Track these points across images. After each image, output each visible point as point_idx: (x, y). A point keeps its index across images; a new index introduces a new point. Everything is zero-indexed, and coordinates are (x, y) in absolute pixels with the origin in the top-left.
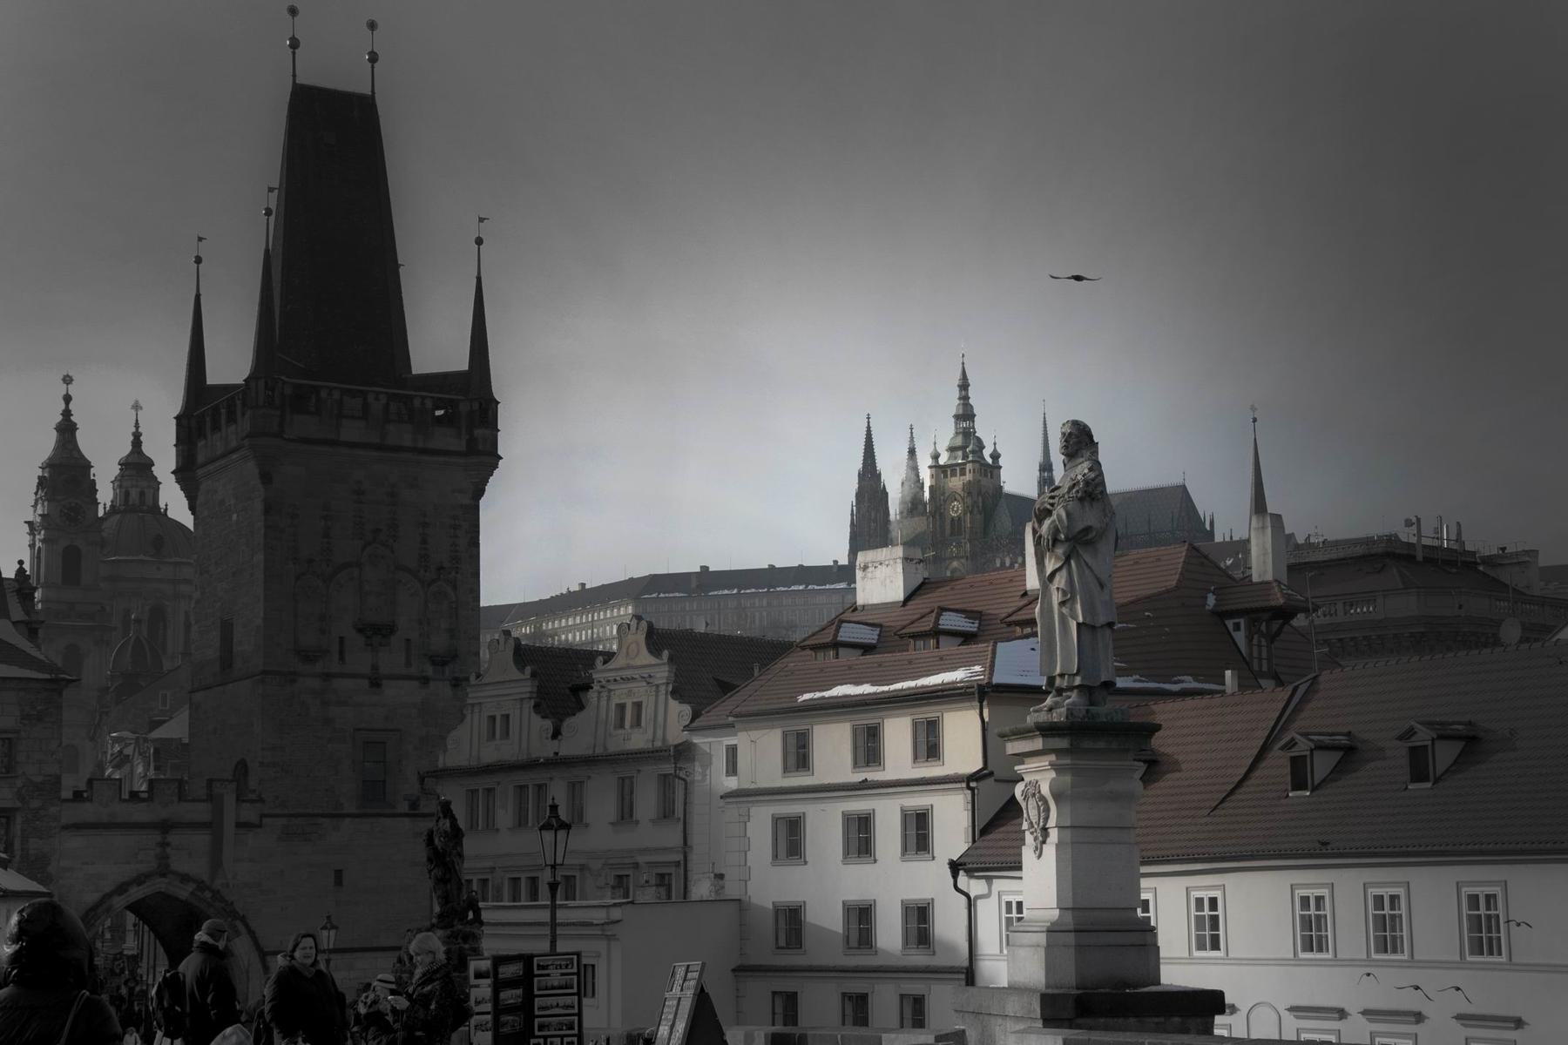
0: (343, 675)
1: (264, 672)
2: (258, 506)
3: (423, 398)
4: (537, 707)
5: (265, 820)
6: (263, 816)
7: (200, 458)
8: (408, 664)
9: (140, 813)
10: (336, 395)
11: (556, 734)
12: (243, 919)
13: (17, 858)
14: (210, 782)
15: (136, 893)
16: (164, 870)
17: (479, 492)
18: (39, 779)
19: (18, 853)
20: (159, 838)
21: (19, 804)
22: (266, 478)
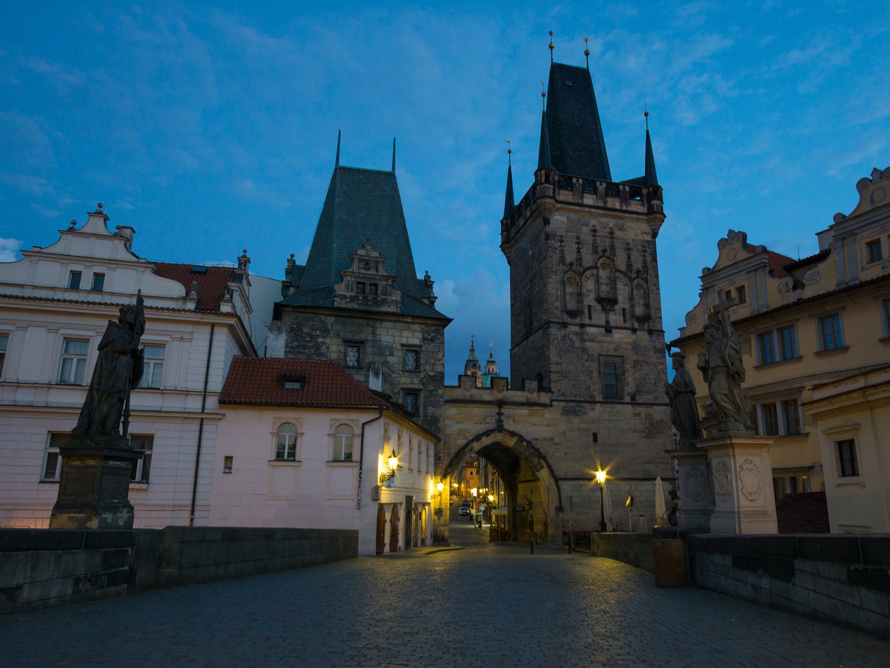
0: (591, 326)
1: (549, 322)
2: (543, 237)
4: (771, 272)
5: (555, 403)
6: (552, 401)
7: (513, 234)
8: (625, 321)
9: (487, 396)
10: (581, 181)
11: (798, 285)
12: (544, 458)
13: (422, 418)
15: (486, 441)
16: (500, 428)
17: (655, 235)
18: (432, 374)
19: (422, 415)
20: (497, 410)
21: (422, 387)
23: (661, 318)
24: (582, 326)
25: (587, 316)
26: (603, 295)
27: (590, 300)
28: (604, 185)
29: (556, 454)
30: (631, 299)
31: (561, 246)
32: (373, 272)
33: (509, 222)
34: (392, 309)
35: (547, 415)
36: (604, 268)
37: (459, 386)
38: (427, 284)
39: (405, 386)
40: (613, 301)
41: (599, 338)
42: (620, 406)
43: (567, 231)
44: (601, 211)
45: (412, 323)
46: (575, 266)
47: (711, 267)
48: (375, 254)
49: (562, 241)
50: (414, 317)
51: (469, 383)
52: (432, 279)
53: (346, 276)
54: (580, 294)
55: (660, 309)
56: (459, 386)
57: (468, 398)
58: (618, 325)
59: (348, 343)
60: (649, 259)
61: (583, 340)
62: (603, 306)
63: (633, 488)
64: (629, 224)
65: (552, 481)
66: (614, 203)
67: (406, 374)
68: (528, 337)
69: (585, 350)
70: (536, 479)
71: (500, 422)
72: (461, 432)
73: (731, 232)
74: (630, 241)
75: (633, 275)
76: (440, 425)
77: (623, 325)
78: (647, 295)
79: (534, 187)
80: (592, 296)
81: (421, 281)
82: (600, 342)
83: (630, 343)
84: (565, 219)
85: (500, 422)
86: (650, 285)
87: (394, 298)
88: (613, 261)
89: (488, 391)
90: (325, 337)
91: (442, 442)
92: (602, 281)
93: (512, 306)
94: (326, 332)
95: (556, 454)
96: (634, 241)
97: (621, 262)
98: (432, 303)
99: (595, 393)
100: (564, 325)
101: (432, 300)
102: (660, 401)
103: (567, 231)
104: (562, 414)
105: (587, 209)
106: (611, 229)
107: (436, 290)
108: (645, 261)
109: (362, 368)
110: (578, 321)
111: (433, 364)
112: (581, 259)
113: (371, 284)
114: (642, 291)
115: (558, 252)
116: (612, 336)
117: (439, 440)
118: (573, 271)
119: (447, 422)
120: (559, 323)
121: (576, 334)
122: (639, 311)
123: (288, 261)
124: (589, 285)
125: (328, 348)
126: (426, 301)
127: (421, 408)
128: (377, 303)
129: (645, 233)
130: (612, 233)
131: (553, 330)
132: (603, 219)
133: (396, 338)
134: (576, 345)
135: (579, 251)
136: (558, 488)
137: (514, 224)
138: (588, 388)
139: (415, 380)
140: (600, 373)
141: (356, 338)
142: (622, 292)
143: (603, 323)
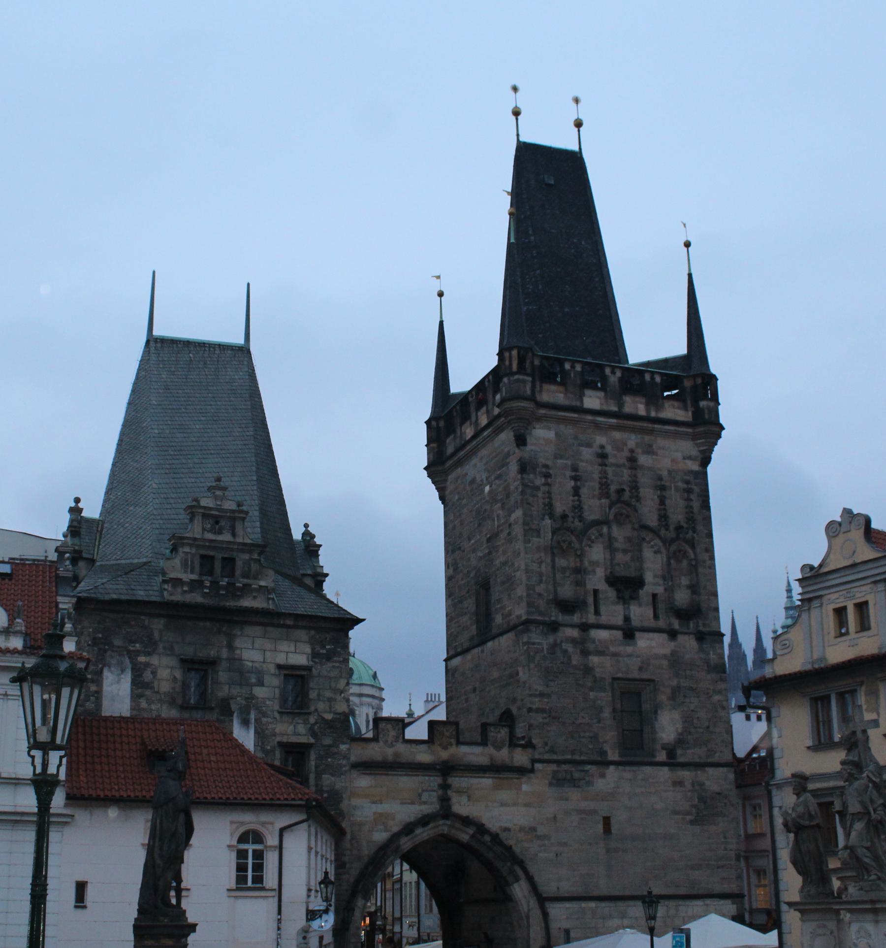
1: (527, 622)
2: (514, 467)
3: (652, 373)
5: (538, 766)
6: (534, 761)
7: (450, 450)
8: (656, 617)
9: (424, 756)
10: (578, 368)
12: (521, 863)
14: (485, 727)
15: (422, 834)
16: (445, 812)
17: (706, 460)
18: (328, 716)
20: (439, 780)
22: (521, 441)
23: (717, 609)
24: (585, 627)
25: (592, 609)
26: (621, 572)
27: (597, 580)
28: (619, 374)
29: (541, 855)
30: (667, 576)
31: (547, 484)
32: (226, 537)
33: (442, 423)
34: (258, 603)
35: (525, 787)
36: (620, 524)
37: (375, 739)
38: (310, 546)
39: (285, 739)
40: (637, 583)
41: (612, 649)
42: (648, 770)
43: (557, 457)
44: (613, 421)
45: (296, 627)
46: (570, 519)
47: (816, 565)
48: (230, 505)
49: (547, 476)
50: (297, 617)
51: (393, 733)
52: (317, 541)
53: (183, 545)
54: (578, 571)
55: (715, 594)
56: (375, 739)
57: (390, 758)
58: (646, 624)
59: (189, 664)
60: (696, 505)
61: (585, 653)
62: (618, 591)
63: (672, 912)
64: (661, 442)
65: (533, 903)
66: (636, 406)
67: (285, 718)
68: (483, 643)
69: (588, 670)
70: (508, 899)
71: (445, 801)
72: (381, 819)
73: (847, 512)
74: (665, 473)
75: (671, 534)
76: (344, 806)
77: (652, 623)
78: (694, 568)
79: (495, 375)
80: (600, 572)
81: (298, 542)
82: (615, 655)
83: (665, 656)
84: (551, 435)
85: (445, 801)
86: (698, 550)
87: (263, 583)
88: (636, 511)
89: (423, 747)
90: (148, 654)
91: (348, 837)
92: (616, 545)
93: (449, 579)
94: (151, 646)
95: (542, 855)
96: (670, 472)
97: (649, 511)
98: (319, 584)
99: (606, 747)
100: (554, 627)
101: (319, 578)
102: (716, 758)
103: (557, 457)
104: (550, 784)
105: (589, 417)
106: (632, 451)
107: (325, 560)
108: (689, 508)
109: (212, 709)
110: (576, 618)
111: (330, 700)
112: (578, 508)
113: (224, 559)
114: (685, 563)
115: (540, 494)
116: (635, 644)
117: (343, 832)
118: (568, 529)
119: (355, 802)
120: (544, 623)
121: (573, 641)
122: (682, 597)
123: (71, 510)
124: (597, 553)
125: (154, 673)
126: (309, 581)
127: (312, 777)
128: (234, 591)
129: (690, 458)
130: (632, 460)
131: (536, 636)
132: (617, 435)
133: (268, 654)
134: (574, 662)
135: (576, 491)
136: (545, 915)
137: (454, 431)
138: (595, 738)
139: (301, 728)
140: (614, 710)
141: (201, 654)
142: (653, 564)
143: (620, 621)
